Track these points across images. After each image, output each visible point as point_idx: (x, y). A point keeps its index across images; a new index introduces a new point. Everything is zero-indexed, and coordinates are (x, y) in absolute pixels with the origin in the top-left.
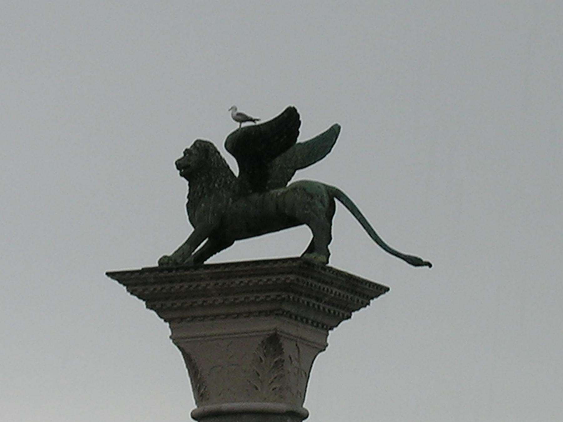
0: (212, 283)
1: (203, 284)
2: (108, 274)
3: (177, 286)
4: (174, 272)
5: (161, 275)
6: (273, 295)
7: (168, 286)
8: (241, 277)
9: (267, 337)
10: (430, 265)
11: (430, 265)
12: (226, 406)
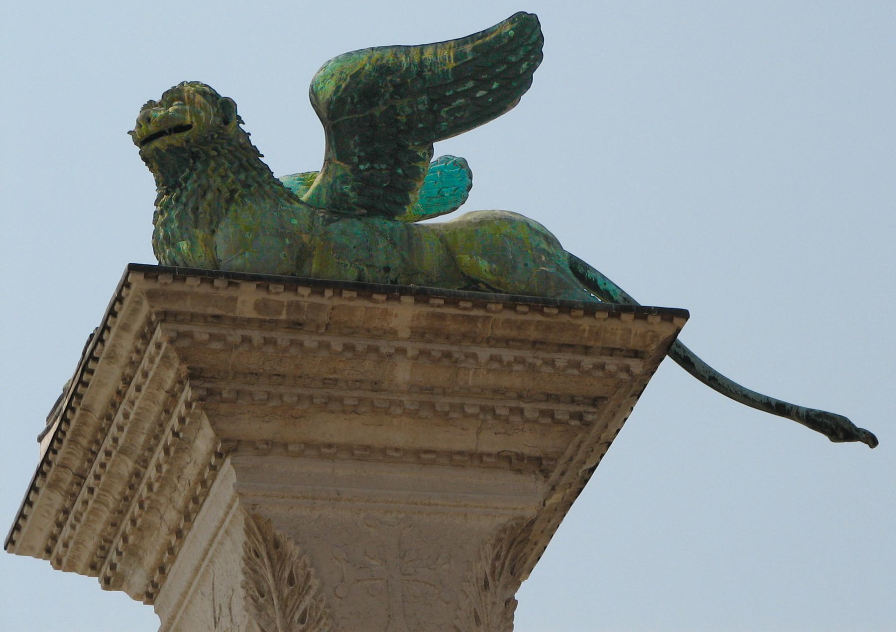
0: (412, 349)
1: (385, 347)
3: (310, 342)
4: (328, 293)
5: (286, 297)
6: (562, 411)
7: (283, 337)
9: (514, 523)
11: (871, 440)
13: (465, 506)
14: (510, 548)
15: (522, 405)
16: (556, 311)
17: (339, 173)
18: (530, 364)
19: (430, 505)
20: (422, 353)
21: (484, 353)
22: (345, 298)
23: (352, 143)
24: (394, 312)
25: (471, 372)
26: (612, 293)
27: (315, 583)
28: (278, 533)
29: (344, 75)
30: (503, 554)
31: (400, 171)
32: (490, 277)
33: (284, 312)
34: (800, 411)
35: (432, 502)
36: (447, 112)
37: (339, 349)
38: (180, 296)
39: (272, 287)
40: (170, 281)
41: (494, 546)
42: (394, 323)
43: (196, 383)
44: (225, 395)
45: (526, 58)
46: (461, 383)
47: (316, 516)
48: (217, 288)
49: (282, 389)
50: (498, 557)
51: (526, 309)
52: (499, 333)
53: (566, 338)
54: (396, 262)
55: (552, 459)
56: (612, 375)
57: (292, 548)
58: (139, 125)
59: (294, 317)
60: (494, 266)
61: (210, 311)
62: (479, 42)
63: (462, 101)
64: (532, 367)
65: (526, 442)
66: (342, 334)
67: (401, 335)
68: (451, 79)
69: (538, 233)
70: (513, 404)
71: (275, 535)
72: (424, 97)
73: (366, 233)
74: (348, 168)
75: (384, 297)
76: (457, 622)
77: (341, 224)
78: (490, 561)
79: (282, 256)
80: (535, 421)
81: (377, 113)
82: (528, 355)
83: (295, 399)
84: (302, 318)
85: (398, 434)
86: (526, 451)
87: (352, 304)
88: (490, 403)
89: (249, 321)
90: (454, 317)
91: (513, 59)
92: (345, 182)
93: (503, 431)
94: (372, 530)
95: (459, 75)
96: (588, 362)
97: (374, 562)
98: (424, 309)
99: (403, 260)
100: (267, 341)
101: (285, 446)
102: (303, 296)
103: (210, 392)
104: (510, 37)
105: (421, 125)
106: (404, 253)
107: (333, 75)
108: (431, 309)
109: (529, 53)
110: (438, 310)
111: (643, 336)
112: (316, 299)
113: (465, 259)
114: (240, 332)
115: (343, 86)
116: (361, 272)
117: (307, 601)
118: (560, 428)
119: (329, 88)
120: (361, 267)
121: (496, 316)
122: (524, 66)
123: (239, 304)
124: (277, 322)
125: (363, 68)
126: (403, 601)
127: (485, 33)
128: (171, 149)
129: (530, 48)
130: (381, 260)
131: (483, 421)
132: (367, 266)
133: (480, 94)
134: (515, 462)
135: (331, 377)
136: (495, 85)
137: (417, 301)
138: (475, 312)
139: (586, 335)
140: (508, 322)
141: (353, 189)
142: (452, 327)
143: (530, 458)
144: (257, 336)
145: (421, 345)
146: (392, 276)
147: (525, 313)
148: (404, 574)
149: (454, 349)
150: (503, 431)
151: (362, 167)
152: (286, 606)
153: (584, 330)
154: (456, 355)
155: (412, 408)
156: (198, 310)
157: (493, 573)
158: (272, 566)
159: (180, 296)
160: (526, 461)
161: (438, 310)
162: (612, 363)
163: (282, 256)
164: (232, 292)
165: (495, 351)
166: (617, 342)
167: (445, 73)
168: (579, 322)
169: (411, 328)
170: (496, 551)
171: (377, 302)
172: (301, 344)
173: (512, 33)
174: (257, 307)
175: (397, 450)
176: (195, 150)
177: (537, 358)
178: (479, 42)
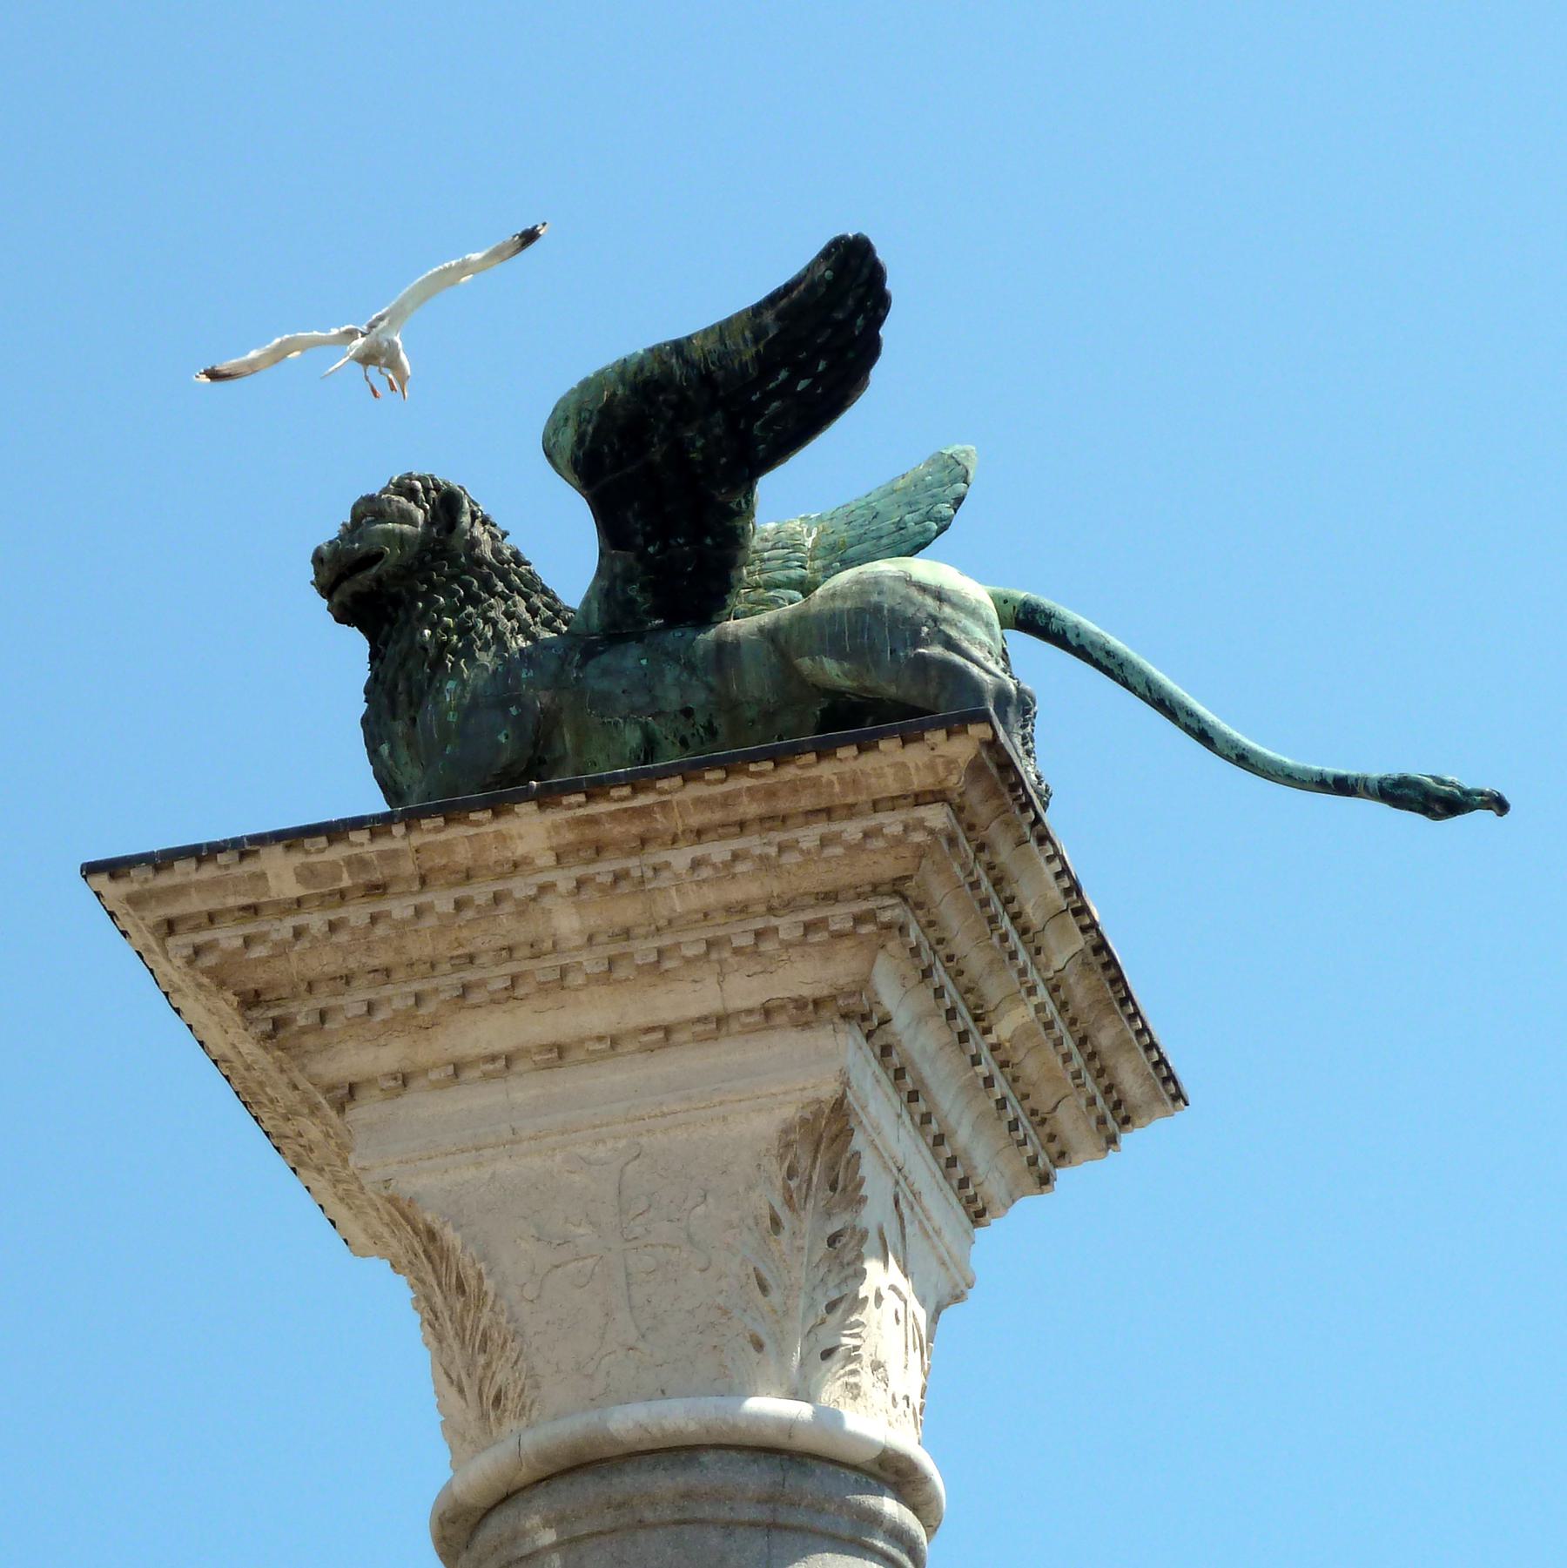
0: (564, 880)
1: (521, 887)
2: (90, 870)
3: (400, 909)
4: (398, 830)
5: (339, 852)
6: (840, 916)
7: (356, 913)
8: (699, 834)
10: (1499, 805)
11: (1499, 805)
12: (628, 1420)
13: (721, 1103)
14: (817, 1151)
15: (774, 921)
16: (769, 765)
17: (618, 567)
18: (761, 857)
19: (664, 1115)
20: (580, 884)
21: (681, 858)
22: (429, 831)
23: (630, 514)
24: (514, 832)
25: (673, 892)
26: (1089, 649)
27: (489, 1284)
28: (429, 1217)
29: (585, 415)
30: (805, 1162)
31: (709, 541)
32: (848, 683)
33: (345, 875)
34: (1370, 784)
35: (665, 1110)
36: (763, 427)
37: (450, 908)
38: (179, 891)
39: (307, 842)
40: (151, 876)
41: (782, 1157)
42: (520, 849)
43: (255, 1013)
44: (301, 1021)
45: (860, 307)
46: (666, 913)
47: (487, 1176)
48: (227, 867)
49: (388, 990)
50: (791, 1173)
51: (720, 774)
52: (696, 820)
53: (806, 801)
54: (698, 697)
55: (852, 994)
56: (898, 841)
57: (451, 1237)
58: (317, 573)
59: (363, 878)
60: (846, 665)
61: (232, 901)
62: (784, 303)
63: (775, 404)
64: (763, 858)
65: (803, 976)
66: (452, 885)
67: (540, 862)
68: (752, 371)
69: (923, 588)
70: (759, 924)
71: (425, 1224)
72: (719, 415)
73: (644, 662)
74: (631, 555)
75: (488, 814)
76: (720, 1300)
77: (605, 659)
78: (779, 1183)
79: (502, 739)
80: (802, 942)
81: (658, 458)
82: (753, 843)
83: (411, 1001)
84: (376, 876)
85: (593, 1014)
86: (807, 992)
87: (442, 837)
88: (720, 932)
89: (299, 902)
90: (613, 816)
91: (840, 316)
92: (629, 581)
93: (758, 968)
94: (576, 1178)
95: (766, 364)
96: (852, 830)
97: (581, 1231)
98: (557, 816)
99: (711, 689)
100: (333, 927)
101: (426, 1071)
102: (362, 845)
103: (278, 1024)
104: (828, 283)
105: (723, 460)
106: (710, 679)
107: (567, 419)
108: (570, 814)
109: (860, 302)
110: (581, 812)
111: (931, 767)
112: (384, 844)
113: (805, 664)
114: (290, 922)
115: (590, 429)
116: (645, 728)
117: (486, 1318)
118: (848, 943)
119: (568, 436)
120: (643, 720)
121: (677, 797)
122: (860, 321)
123: (272, 882)
124: (342, 894)
125: (614, 394)
126: (628, 1285)
127: (788, 288)
128: (357, 598)
129: (861, 290)
130: (672, 699)
131: (721, 962)
132: (654, 716)
133: (802, 385)
134: (809, 1011)
135: (456, 953)
136: (822, 366)
137: (542, 806)
138: (643, 800)
139: (837, 788)
140: (699, 802)
141: (643, 589)
142: (615, 830)
143: (817, 1003)
144: (316, 921)
145: (579, 871)
146: (700, 719)
147: (722, 781)
148: (627, 1240)
149: (632, 863)
150: (758, 968)
151: (651, 549)
152: (464, 1330)
153: (830, 784)
154: (636, 873)
155: (596, 970)
156: (213, 904)
157: (789, 1201)
158: (435, 1270)
159: (179, 891)
160: (811, 1007)
161: (581, 812)
162: (892, 823)
163: (502, 739)
164: (249, 866)
165: (699, 851)
166: (894, 788)
167: (744, 366)
168: (814, 772)
169: (551, 848)
170: (786, 1165)
171: (478, 824)
172: (388, 914)
173: (828, 273)
174: (306, 874)
175: (600, 1039)
176: (394, 590)
177: (769, 844)
178: (784, 303)
